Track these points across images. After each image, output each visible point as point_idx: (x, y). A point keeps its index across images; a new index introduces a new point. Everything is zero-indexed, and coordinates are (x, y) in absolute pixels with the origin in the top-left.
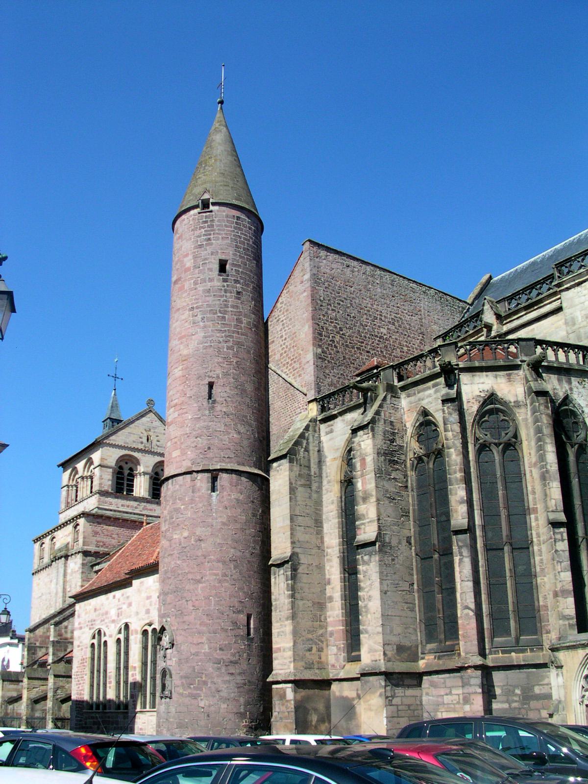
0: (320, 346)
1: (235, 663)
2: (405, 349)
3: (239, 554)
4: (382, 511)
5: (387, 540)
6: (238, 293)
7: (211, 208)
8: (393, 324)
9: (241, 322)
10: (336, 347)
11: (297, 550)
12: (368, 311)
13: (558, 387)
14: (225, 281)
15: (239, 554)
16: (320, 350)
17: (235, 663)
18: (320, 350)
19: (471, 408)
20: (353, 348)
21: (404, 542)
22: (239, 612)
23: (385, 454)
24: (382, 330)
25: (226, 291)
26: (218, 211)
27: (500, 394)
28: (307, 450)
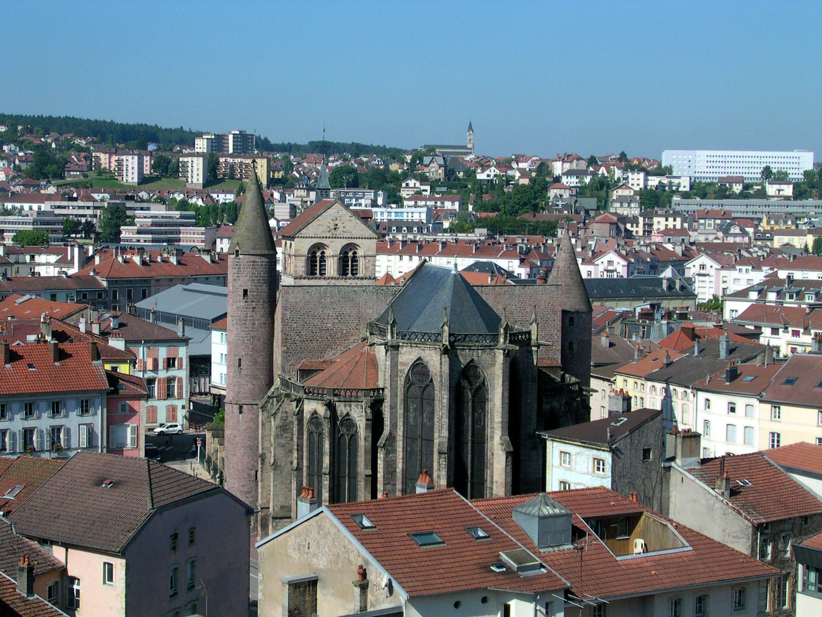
0: (285, 346)
1: (249, 492)
2: (345, 331)
3: (251, 443)
4: (276, 452)
5: (279, 464)
6: (253, 308)
7: (240, 256)
8: (337, 318)
9: (255, 325)
10: (296, 343)
11: (265, 452)
12: (320, 316)
14: (246, 302)
15: (251, 443)
16: (285, 348)
17: (249, 492)
18: (285, 348)
19: (307, 416)
20: (307, 341)
21: (289, 463)
22: (251, 470)
23: (281, 427)
24: (328, 325)
25: (247, 308)
26: (243, 259)
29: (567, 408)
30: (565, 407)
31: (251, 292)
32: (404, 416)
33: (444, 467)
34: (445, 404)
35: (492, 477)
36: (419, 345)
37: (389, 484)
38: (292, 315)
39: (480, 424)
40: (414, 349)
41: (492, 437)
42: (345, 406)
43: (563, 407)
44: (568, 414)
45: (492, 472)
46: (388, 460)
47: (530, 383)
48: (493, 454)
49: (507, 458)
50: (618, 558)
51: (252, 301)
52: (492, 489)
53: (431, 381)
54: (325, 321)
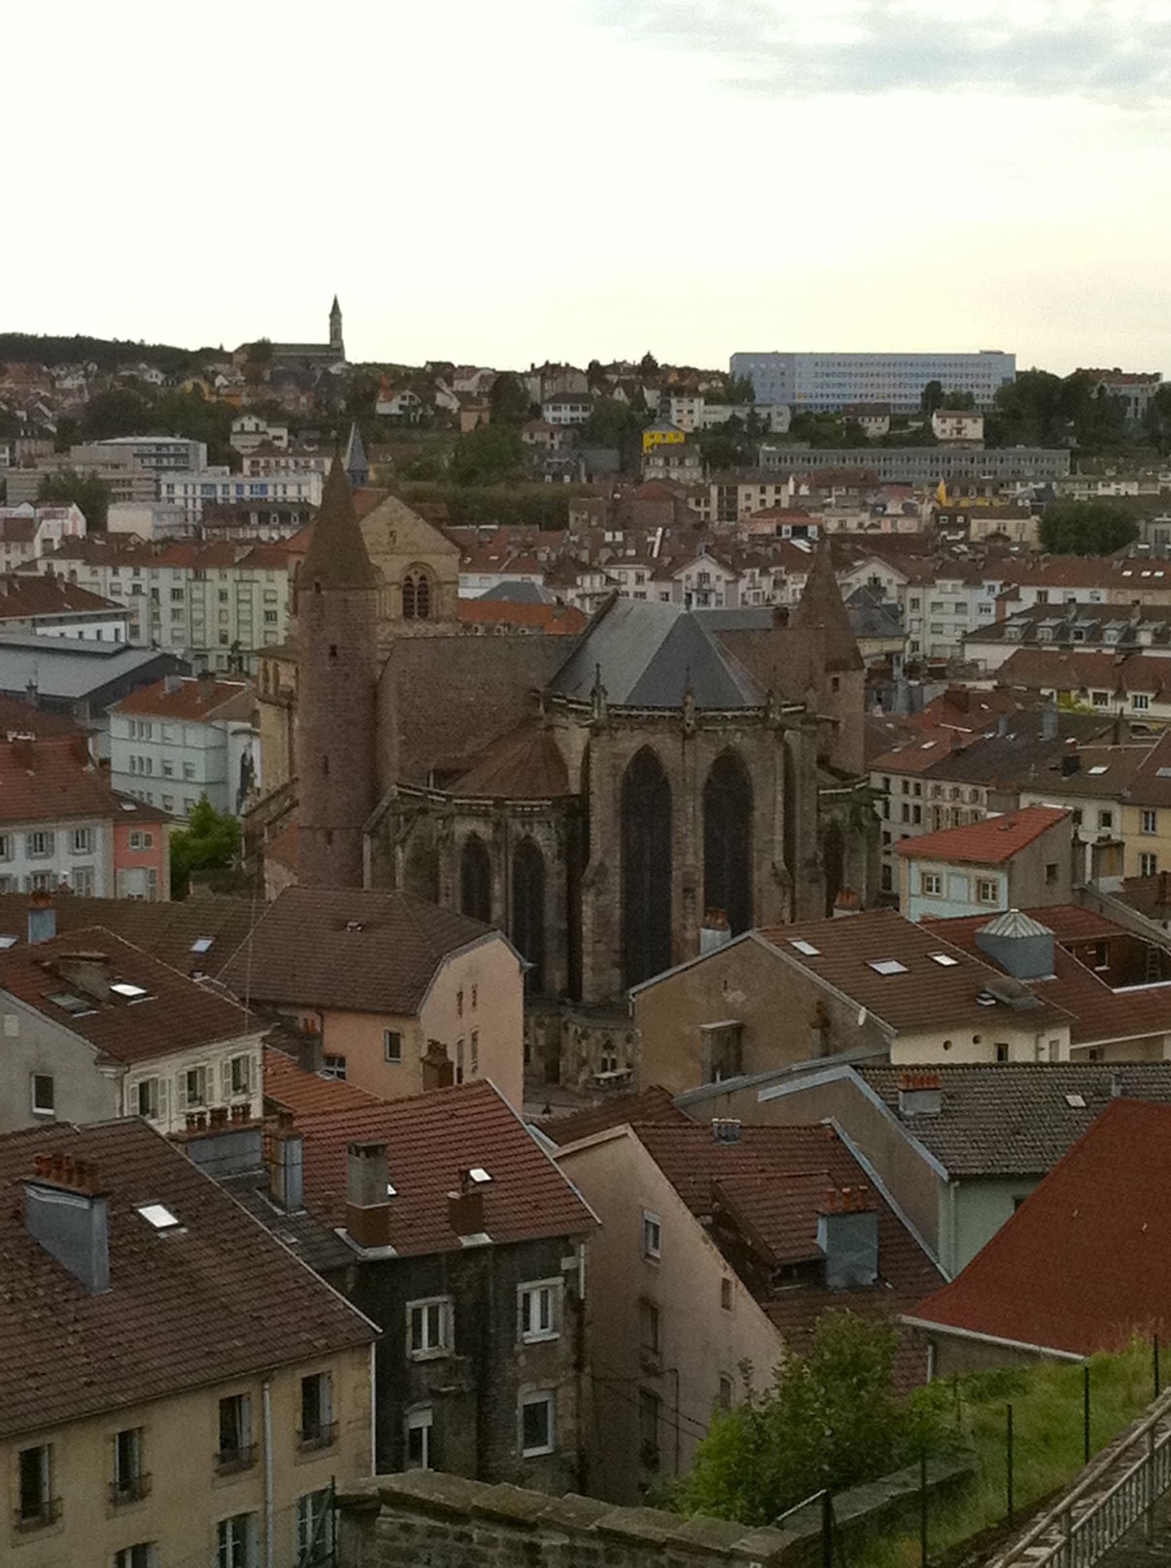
6: (347, 675)
7: (323, 592)
14: (334, 665)
27: (478, 833)
28: (387, 825)
37: (598, 942)
40: (636, 732)
49: (784, 894)
50: (1116, 991)
53: (666, 781)
54: (465, 693)
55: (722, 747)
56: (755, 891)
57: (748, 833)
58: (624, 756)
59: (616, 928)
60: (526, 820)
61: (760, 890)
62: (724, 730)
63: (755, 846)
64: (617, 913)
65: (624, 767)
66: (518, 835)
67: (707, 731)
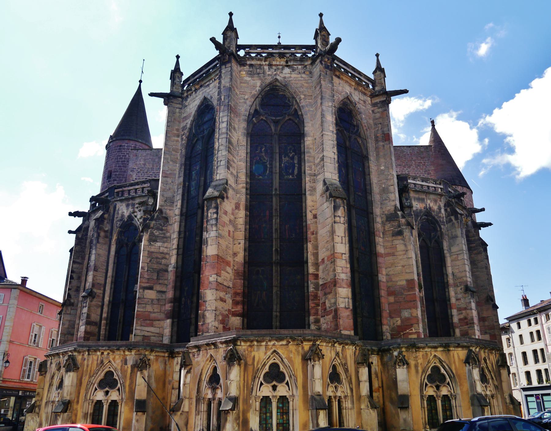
13: (125, 211)
14: (109, 181)
29: (449, 210)
30: (446, 210)
31: (115, 172)
32: (184, 186)
33: (214, 222)
34: (224, 130)
35: (316, 255)
36: (203, 83)
37: (151, 288)
38: (139, 176)
39: (292, 174)
41: (314, 189)
42: (128, 206)
43: (443, 211)
44: (453, 218)
45: (316, 247)
46: (152, 250)
47: (381, 143)
48: (315, 217)
49: (336, 208)
51: (114, 180)
52: (316, 276)
55: (269, 80)
56: (309, 216)
57: (301, 161)
58: (189, 116)
59: (171, 276)
60: (131, 202)
61: (315, 217)
62: (270, 65)
63: (308, 172)
64: (173, 260)
65: (188, 126)
66: (123, 216)
67: (251, 65)
